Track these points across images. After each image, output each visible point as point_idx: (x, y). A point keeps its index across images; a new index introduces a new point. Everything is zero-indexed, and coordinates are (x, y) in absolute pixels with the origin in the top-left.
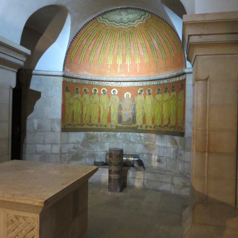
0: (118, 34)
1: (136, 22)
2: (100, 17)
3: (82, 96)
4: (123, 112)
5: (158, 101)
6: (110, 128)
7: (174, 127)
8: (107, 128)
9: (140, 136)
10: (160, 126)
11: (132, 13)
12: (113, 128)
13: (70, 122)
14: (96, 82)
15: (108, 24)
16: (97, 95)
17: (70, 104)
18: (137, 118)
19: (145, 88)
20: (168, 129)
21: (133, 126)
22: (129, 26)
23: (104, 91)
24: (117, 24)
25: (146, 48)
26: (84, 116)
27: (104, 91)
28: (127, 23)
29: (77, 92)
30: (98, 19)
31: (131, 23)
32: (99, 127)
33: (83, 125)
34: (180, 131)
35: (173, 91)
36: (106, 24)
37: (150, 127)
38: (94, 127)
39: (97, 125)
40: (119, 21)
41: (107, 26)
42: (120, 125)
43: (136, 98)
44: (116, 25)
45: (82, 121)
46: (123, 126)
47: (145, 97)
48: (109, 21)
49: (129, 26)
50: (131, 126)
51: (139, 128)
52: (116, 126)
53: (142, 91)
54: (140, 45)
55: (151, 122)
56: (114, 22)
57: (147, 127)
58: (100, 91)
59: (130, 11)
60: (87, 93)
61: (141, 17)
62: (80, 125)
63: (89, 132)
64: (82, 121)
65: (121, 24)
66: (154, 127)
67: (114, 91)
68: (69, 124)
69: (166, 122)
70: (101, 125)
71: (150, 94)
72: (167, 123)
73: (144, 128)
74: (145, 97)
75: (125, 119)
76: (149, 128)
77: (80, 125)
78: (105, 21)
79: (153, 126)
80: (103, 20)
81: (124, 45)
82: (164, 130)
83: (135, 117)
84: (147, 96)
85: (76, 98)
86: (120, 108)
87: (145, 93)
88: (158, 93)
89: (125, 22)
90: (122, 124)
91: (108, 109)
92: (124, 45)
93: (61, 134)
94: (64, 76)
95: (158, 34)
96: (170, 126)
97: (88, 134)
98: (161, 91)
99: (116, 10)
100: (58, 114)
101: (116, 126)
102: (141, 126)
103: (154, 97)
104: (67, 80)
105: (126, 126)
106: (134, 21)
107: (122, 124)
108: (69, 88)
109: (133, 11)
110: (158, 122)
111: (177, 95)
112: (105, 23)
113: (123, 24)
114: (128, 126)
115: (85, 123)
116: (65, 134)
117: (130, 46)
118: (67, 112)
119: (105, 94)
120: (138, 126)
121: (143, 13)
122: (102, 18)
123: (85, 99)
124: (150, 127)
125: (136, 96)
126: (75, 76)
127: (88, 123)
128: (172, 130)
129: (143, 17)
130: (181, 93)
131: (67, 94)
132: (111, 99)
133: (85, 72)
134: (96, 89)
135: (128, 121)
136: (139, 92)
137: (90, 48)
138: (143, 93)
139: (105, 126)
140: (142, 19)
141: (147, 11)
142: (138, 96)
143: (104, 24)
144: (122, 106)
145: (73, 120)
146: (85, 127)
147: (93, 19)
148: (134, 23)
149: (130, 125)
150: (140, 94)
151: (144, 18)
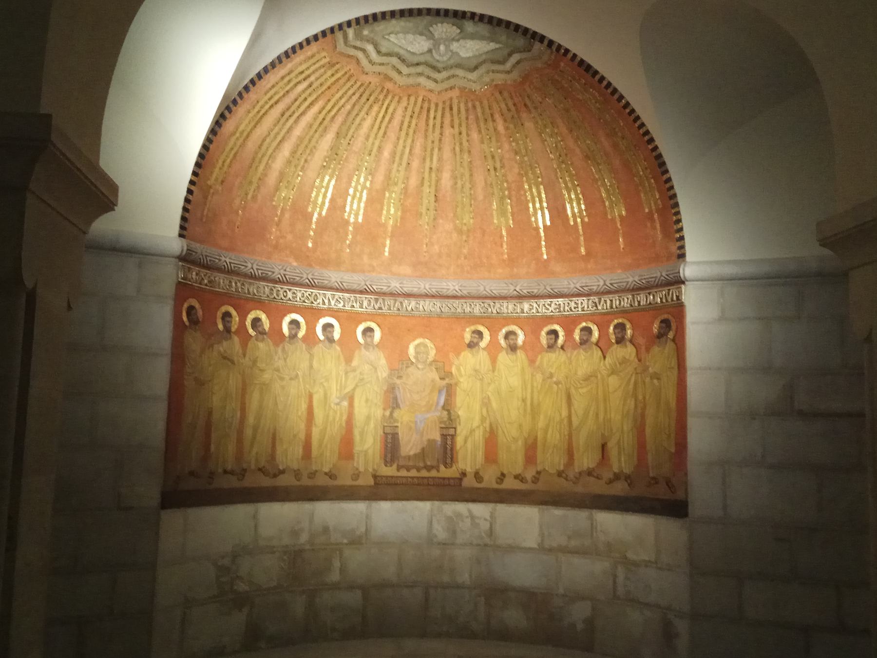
2: (351, 32)
4: (403, 417)
5: (551, 376)
6: (349, 482)
7: (628, 478)
8: (339, 482)
9: (472, 517)
10: (560, 474)
12: (361, 482)
18: (459, 440)
20: (598, 487)
21: (445, 472)
24: (405, 70)
27: (328, 327)
28: (445, 69)
31: (460, 72)
32: (306, 481)
34: (662, 492)
35: (620, 341)
36: (364, 62)
38: (284, 481)
39: (297, 474)
40: (416, 60)
42: (389, 471)
43: (456, 362)
44: (400, 73)
46: (404, 473)
47: (494, 360)
48: (379, 52)
49: (452, 82)
50: (434, 473)
51: (469, 482)
52: (375, 477)
55: (520, 458)
56: (394, 61)
58: (311, 329)
60: (513, 348)
62: (232, 473)
65: (420, 69)
66: (535, 480)
67: (368, 331)
68: (192, 474)
69: (586, 460)
70: (312, 475)
72: (592, 465)
73: (489, 480)
74: (494, 360)
75: (410, 446)
76: (510, 484)
78: (364, 51)
79: (529, 475)
80: (358, 44)
82: (579, 489)
83: (453, 437)
84: (503, 358)
86: (392, 401)
87: (494, 342)
88: (551, 347)
89: (440, 65)
90: (399, 469)
91: (345, 404)
92: (418, 150)
96: (607, 475)
98: (561, 340)
101: (375, 477)
102: (477, 476)
103: (532, 362)
105: (413, 473)
107: (399, 468)
112: (360, 55)
114: (424, 473)
117: (440, 159)
120: (464, 474)
121: (520, 42)
122: (358, 36)
124: (516, 477)
125: (458, 354)
127: (262, 463)
128: (619, 489)
129: (516, 57)
132: (355, 363)
135: (422, 454)
139: (331, 475)
140: (508, 65)
143: (358, 62)
144: (400, 394)
149: (429, 468)
151: (518, 63)
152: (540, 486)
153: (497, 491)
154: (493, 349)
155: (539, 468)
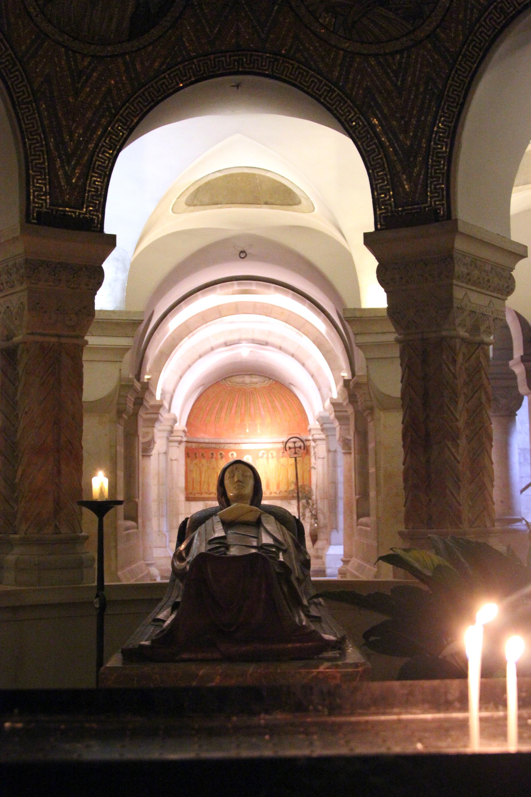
0: (238, 393)
1: (258, 384)
3: (200, 461)
10: (286, 491)
11: (256, 378)
13: (190, 491)
14: (213, 445)
15: (229, 385)
16: (214, 460)
17: (190, 470)
19: (268, 451)
22: (251, 387)
23: (221, 454)
24: (238, 385)
25: (268, 408)
26: (202, 483)
29: (196, 457)
30: (221, 382)
31: (252, 384)
33: (201, 493)
37: (275, 493)
41: (227, 387)
45: (200, 490)
53: (264, 454)
54: (260, 405)
55: (275, 487)
57: (271, 493)
58: (217, 455)
59: (254, 376)
61: (265, 381)
63: (207, 502)
64: (200, 490)
66: (279, 493)
67: (232, 454)
71: (273, 457)
76: (273, 495)
77: (199, 493)
79: (278, 492)
81: (243, 403)
84: (271, 460)
85: (196, 464)
92: (243, 403)
93: (185, 503)
94: (187, 442)
95: (281, 398)
97: (207, 504)
99: (240, 375)
100: (182, 483)
103: (278, 460)
104: (190, 445)
106: (257, 384)
108: (190, 455)
109: (257, 376)
110: (283, 488)
111: (303, 460)
113: (244, 385)
115: (204, 492)
116: (187, 503)
118: (189, 480)
119: (222, 457)
121: (268, 379)
123: (203, 465)
124: (275, 493)
126: (195, 440)
130: (307, 457)
131: (189, 460)
133: (202, 435)
134: (213, 452)
136: (260, 455)
137: (208, 408)
138: (265, 456)
140: (265, 383)
141: (272, 379)
142: (260, 460)
143: (225, 385)
145: (193, 489)
146: (203, 496)
147: (217, 382)
148: (257, 385)
150: (262, 457)
152: (281, 495)
153: (269, 497)
154: (268, 458)
155: (281, 490)
